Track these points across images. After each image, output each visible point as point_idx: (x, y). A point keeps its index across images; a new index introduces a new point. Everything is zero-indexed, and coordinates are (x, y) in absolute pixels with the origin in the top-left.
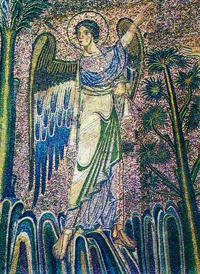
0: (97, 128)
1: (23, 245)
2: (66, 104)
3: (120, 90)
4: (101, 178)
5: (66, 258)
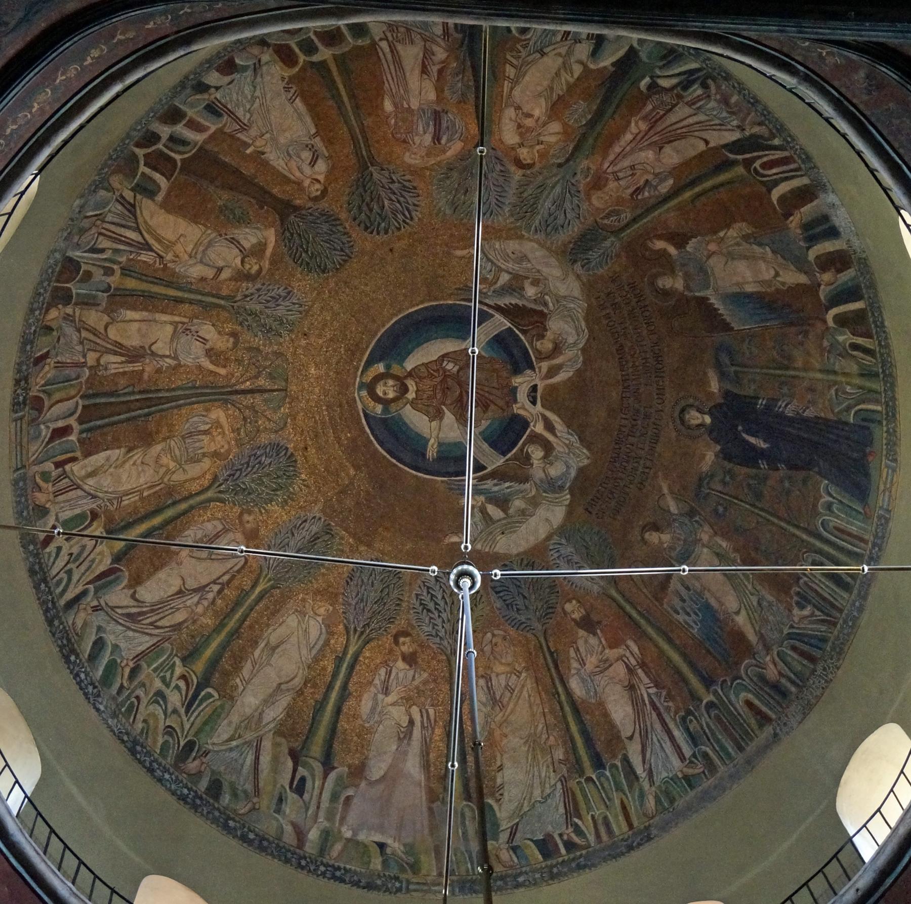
1: (749, 704)
2: (688, 588)
3: (705, 537)
4: (754, 600)
5: (780, 674)
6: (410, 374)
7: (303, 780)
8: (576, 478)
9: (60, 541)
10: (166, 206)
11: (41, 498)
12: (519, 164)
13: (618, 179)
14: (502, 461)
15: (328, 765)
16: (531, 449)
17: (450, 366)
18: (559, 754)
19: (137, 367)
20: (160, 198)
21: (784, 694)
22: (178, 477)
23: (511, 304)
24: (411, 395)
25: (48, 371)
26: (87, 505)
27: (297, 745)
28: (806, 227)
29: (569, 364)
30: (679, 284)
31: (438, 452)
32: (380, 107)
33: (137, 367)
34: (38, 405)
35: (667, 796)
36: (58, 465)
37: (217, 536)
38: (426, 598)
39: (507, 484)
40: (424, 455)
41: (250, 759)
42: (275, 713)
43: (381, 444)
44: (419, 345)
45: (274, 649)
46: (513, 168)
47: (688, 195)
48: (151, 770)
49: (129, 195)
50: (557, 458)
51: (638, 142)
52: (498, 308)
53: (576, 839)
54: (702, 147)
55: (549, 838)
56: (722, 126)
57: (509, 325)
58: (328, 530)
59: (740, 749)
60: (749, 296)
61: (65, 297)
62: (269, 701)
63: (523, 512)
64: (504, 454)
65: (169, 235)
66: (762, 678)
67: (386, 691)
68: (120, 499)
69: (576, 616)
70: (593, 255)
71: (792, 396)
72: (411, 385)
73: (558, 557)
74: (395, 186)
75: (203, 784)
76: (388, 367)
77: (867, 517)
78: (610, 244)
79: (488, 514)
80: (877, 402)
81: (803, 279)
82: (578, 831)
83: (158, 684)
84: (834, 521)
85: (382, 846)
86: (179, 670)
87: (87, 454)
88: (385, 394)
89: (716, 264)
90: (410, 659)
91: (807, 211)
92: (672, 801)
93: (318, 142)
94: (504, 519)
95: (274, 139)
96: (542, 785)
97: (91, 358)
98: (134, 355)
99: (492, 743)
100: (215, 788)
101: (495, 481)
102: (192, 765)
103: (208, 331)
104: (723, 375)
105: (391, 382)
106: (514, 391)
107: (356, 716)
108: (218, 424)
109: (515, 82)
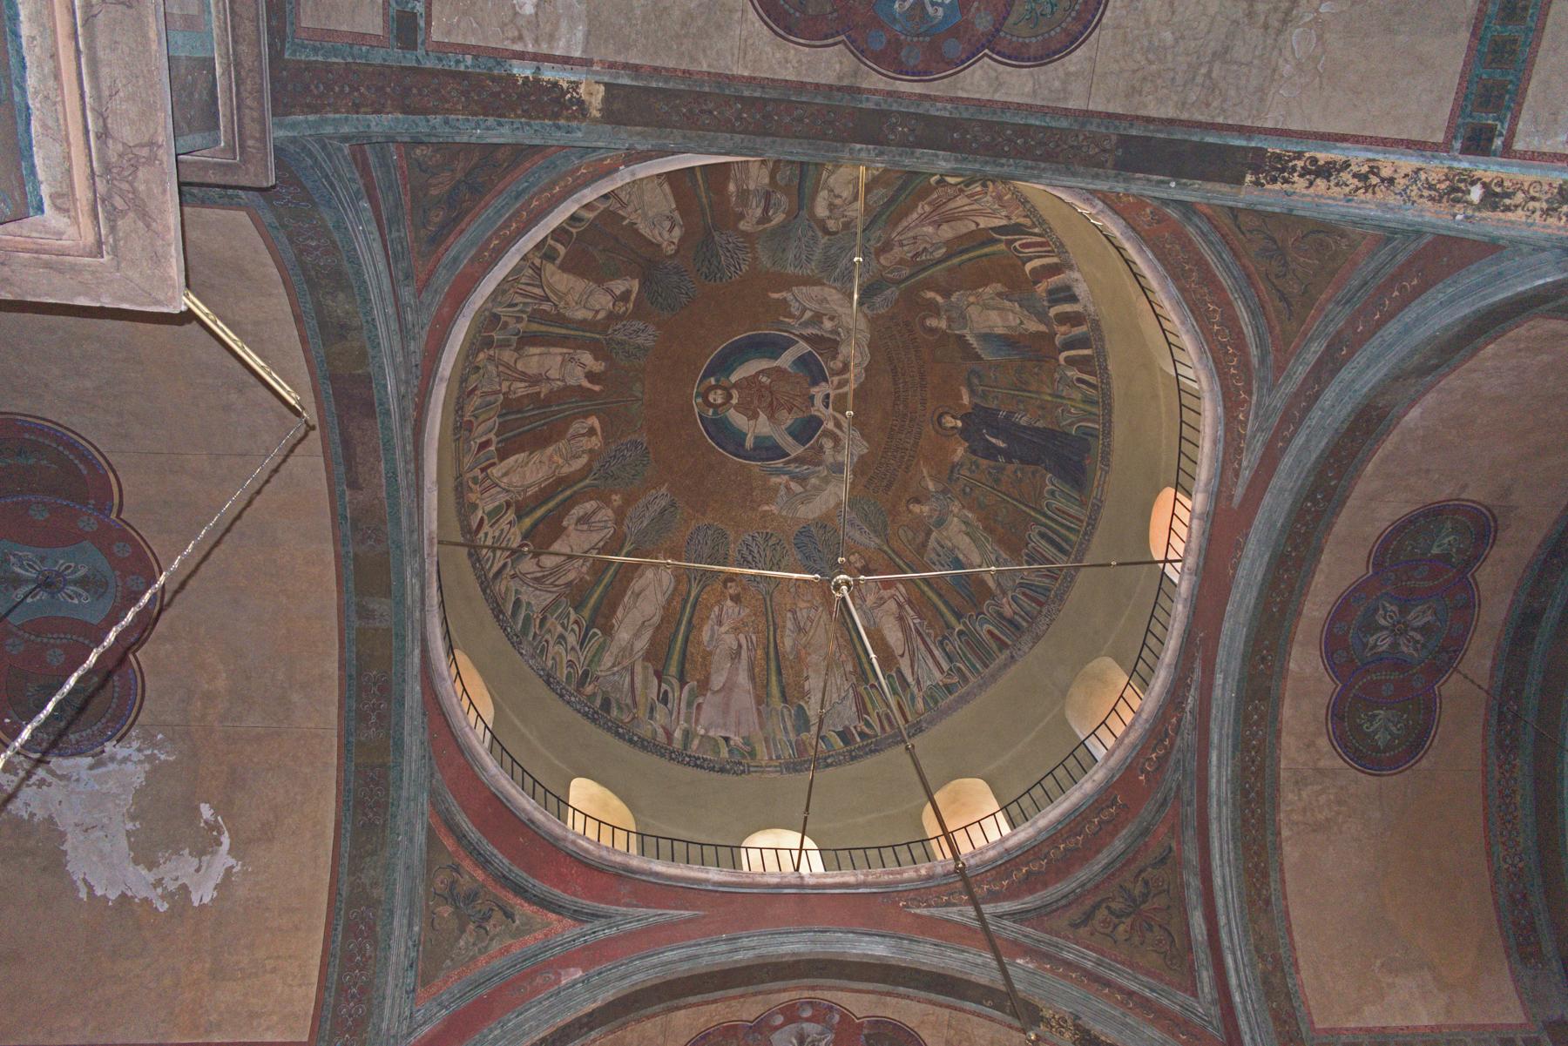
0: (967, 540)
1: (990, 632)
6: (735, 385)
7: (666, 692)
9: (486, 528)
10: (563, 268)
11: (473, 497)
12: (826, 232)
13: (902, 245)
15: (683, 683)
18: (849, 668)
19: (537, 389)
20: (558, 262)
21: (1017, 627)
22: (566, 470)
24: (734, 401)
25: (476, 401)
26: (502, 498)
27: (660, 668)
28: (1050, 292)
29: (854, 378)
30: (943, 324)
32: (726, 187)
33: (537, 389)
34: (469, 426)
35: (931, 698)
36: (483, 470)
37: (594, 513)
38: (745, 551)
40: (742, 445)
41: (628, 679)
42: (642, 644)
45: (638, 595)
46: (820, 234)
47: (956, 261)
48: (562, 696)
49: (537, 262)
51: (923, 220)
52: (802, 337)
53: (867, 730)
54: (973, 227)
55: (847, 728)
56: (993, 214)
58: (673, 504)
59: (986, 666)
60: (999, 336)
61: (488, 343)
62: (637, 635)
63: (815, 487)
65: (561, 288)
66: (1000, 615)
67: (720, 624)
68: (525, 491)
69: (858, 565)
70: (878, 300)
71: (1026, 410)
72: (735, 393)
74: (730, 247)
75: (598, 702)
77: (1082, 504)
78: (892, 293)
80: (1093, 421)
81: (1043, 328)
82: (868, 725)
83: (560, 629)
84: (1055, 504)
85: (727, 739)
86: (573, 616)
87: (502, 459)
89: (973, 312)
90: (736, 599)
91: (1055, 280)
92: (936, 703)
93: (676, 215)
95: (645, 215)
96: (838, 689)
97: (505, 387)
98: (534, 380)
99: (798, 658)
100: (606, 705)
102: (589, 689)
103: (587, 358)
104: (972, 392)
106: (812, 398)
107: (700, 643)
108: (592, 432)
109: (832, 173)
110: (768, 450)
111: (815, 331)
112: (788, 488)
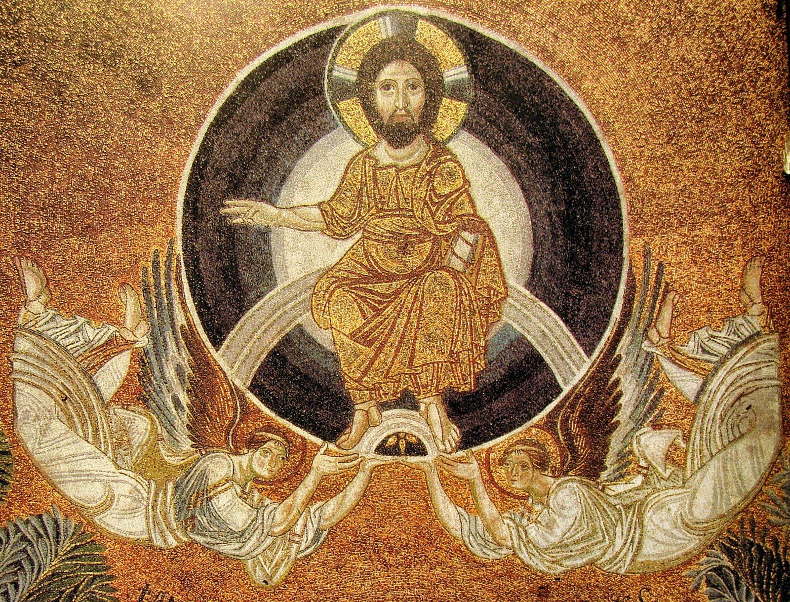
6: (439, 149)
8: (218, 557)
14: (238, 383)
16: (274, 446)
17: (462, 249)
23: (620, 395)
24: (384, 153)
31: (246, 228)
39: (184, 399)
43: (250, 84)
44: (516, 171)
50: (258, 508)
57: (566, 389)
64: (255, 387)
72: (415, 152)
73: (24, 538)
76: (457, 92)
79: (108, 358)
88: (387, 87)
94: (101, 398)
101: (188, 371)
105: (417, 99)
106: (407, 401)
110: (227, 274)
111: (627, 401)
112: (111, 348)
